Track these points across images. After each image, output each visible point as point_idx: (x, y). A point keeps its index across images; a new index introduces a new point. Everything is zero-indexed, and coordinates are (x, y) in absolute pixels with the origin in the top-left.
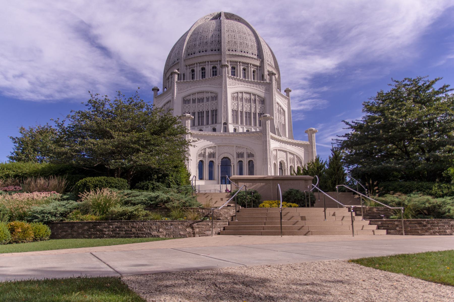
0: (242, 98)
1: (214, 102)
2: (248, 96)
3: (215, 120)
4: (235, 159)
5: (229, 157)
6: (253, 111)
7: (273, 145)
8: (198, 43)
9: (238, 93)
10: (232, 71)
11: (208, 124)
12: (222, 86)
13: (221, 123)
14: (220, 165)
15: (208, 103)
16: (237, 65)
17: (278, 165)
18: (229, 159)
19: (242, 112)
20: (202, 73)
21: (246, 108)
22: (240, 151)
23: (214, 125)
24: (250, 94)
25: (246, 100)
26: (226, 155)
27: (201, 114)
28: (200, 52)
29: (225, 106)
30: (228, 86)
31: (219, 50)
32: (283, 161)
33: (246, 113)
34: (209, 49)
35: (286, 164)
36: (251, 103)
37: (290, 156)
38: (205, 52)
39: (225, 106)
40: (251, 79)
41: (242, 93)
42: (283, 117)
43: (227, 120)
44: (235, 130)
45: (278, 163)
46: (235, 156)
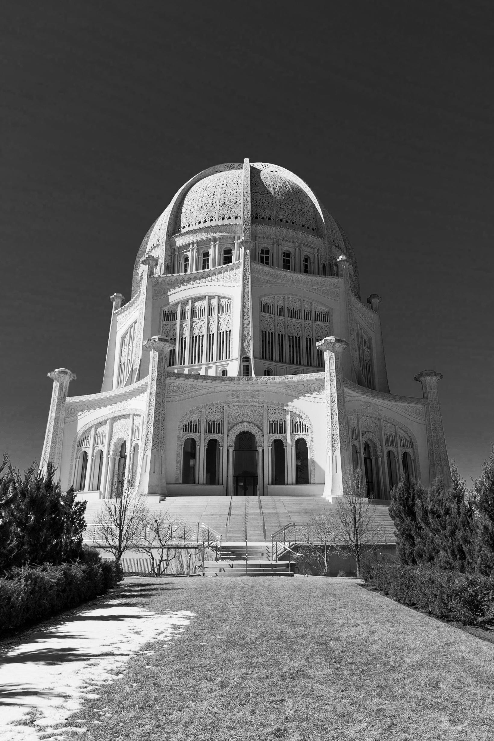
4: (266, 436)
5: (253, 433)
8: (195, 206)
10: (262, 258)
11: (209, 358)
14: (231, 450)
17: (362, 451)
20: (204, 261)
26: (245, 427)
28: (200, 223)
29: (246, 322)
32: (371, 440)
33: (292, 338)
34: (217, 216)
35: (379, 448)
38: (208, 222)
45: (362, 446)
46: (266, 429)
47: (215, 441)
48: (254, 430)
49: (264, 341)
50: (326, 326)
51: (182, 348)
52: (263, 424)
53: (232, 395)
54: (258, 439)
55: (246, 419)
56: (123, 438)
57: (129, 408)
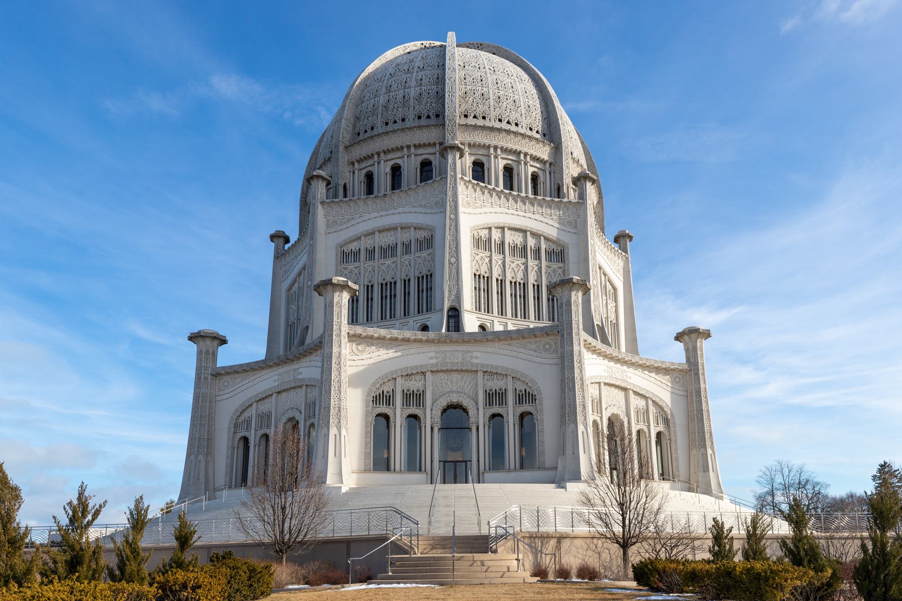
0: (503, 243)
1: (424, 254)
2: (518, 239)
3: (426, 303)
4: (481, 410)
6: (532, 279)
7: (593, 368)
9: (490, 229)
12: (445, 207)
13: (442, 310)
15: (407, 257)
16: (489, 156)
18: (465, 411)
19: (501, 283)
21: (514, 269)
22: (496, 384)
23: (423, 318)
24: (524, 232)
25: (514, 248)
26: (455, 399)
27: (388, 287)
29: (453, 260)
30: (461, 209)
31: (440, 115)
33: (514, 284)
36: (526, 257)
37: (636, 403)
39: (453, 260)
40: (526, 192)
41: (503, 228)
42: (611, 305)
43: (458, 297)
44: (482, 327)
47: (415, 417)
48: (466, 402)
49: (477, 289)
50: (560, 268)
51: (370, 300)
52: (477, 394)
53: (437, 358)
54: (472, 413)
55: (454, 389)
56: (294, 418)
57: (300, 377)
